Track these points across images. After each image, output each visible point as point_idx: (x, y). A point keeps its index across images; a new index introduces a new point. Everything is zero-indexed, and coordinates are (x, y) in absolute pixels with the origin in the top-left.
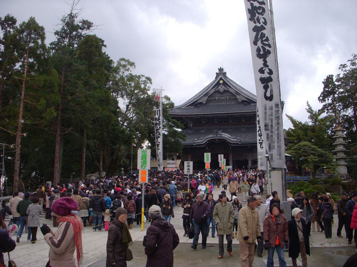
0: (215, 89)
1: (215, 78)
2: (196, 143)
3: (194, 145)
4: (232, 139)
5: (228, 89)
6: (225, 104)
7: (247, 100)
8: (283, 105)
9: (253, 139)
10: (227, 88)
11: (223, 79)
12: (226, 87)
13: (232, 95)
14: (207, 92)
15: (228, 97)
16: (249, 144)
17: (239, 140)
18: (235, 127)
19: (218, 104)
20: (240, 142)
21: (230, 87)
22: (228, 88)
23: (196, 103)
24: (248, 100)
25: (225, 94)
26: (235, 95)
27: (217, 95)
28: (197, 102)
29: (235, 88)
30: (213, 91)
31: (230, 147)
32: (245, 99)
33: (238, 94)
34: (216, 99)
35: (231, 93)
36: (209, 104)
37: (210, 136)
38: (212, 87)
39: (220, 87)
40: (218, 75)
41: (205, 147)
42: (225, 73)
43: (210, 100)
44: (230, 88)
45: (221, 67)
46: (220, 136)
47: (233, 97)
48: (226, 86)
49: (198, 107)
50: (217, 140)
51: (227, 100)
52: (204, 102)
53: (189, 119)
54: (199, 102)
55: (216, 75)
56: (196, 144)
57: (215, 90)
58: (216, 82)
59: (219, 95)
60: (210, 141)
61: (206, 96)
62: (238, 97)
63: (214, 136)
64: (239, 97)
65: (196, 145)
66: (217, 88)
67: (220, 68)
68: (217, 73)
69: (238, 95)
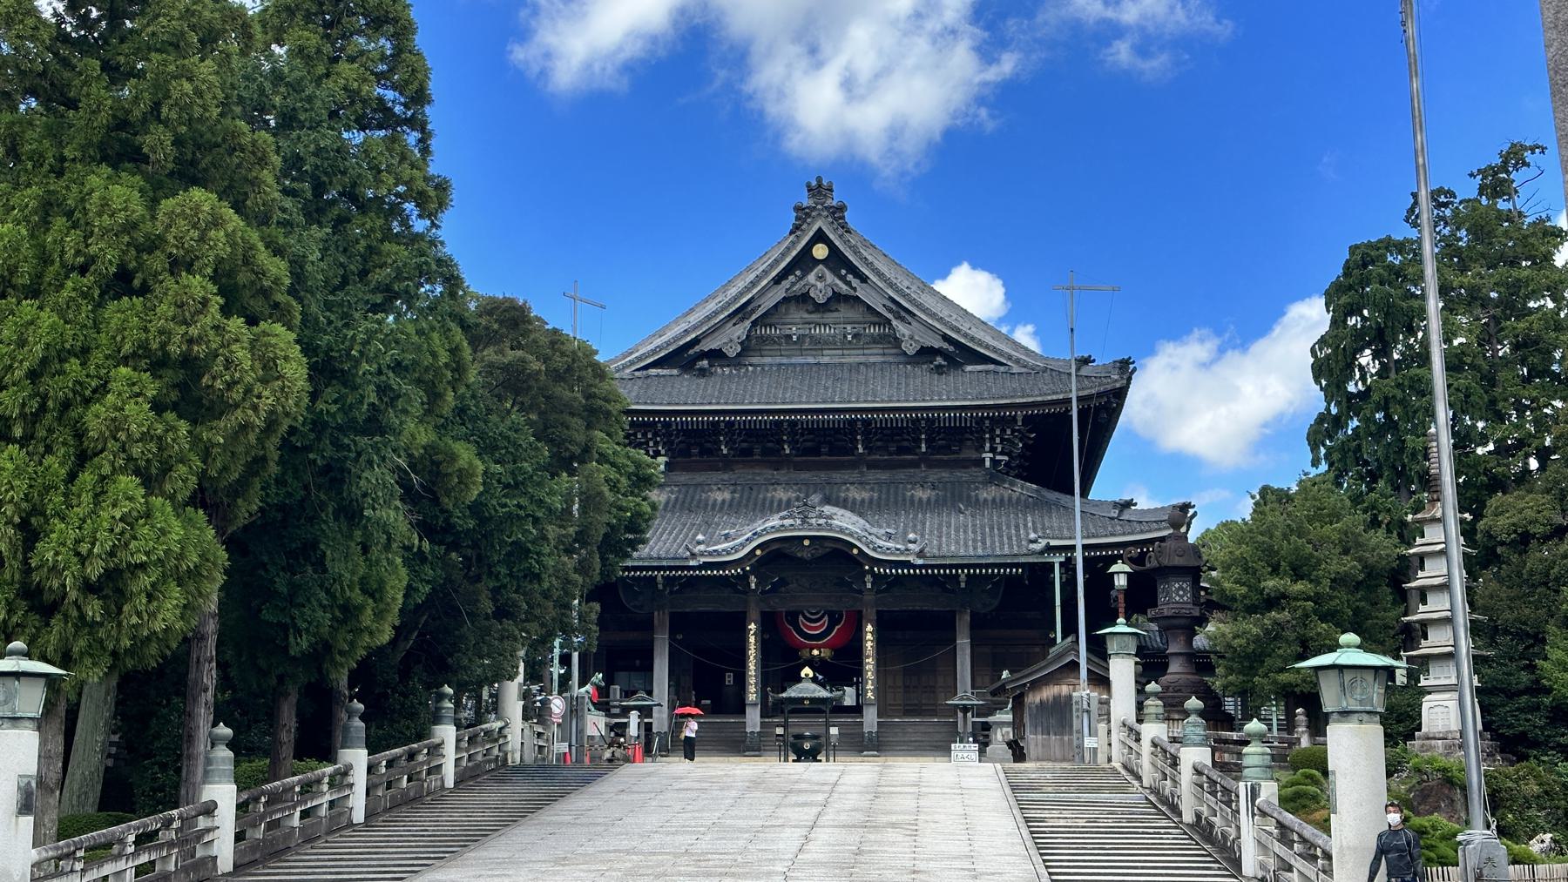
0: (786, 284)
1: (791, 233)
2: (702, 554)
3: (692, 563)
4: (881, 543)
6: (837, 360)
7: (945, 346)
8: (1129, 379)
9: (984, 543)
10: (848, 284)
11: (832, 237)
13: (876, 319)
15: (849, 328)
16: (962, 566)
17: (911, 546)
18: (884, 476)
19: (800, 360)
20: (921, 554)
21: (864, 279)
22: (855, 282)
23: (691, 352)
24: (951, 349)
25: (835, 314)
27: (797, 314)
28: (697, 349)
29: (891, 285)
30: (779, 293)
31: (868, 578)
32: (938, 343)
33: (902, 313)
34: (789, 337)
35: (869, 307)
36: (755, 360)
37: (774, 525)
38: (774, 274)
39: (811, 278)
40: (803, 214)
41: (744, 577)
42: (841, 208)
43: (764, 340)
45: (819, 179)
46: (822, 521)
47: (874, 331)
48: (843, 272)
49: (703, 373)
50: (806, 543)
51: (844, 345)
52: (732, 351)
53: (655, 434)
54: (707, 346)
55: (797, 218)
56: (703, 560)
58: (794, 253)
61: (742, 320)
62: (901, 328)
63: (790, 521)
64: (907, 333)
65: (700, 567)
66: (801, 279)
67: (814, 183)
68: (798, 209)
69: (902, 319)
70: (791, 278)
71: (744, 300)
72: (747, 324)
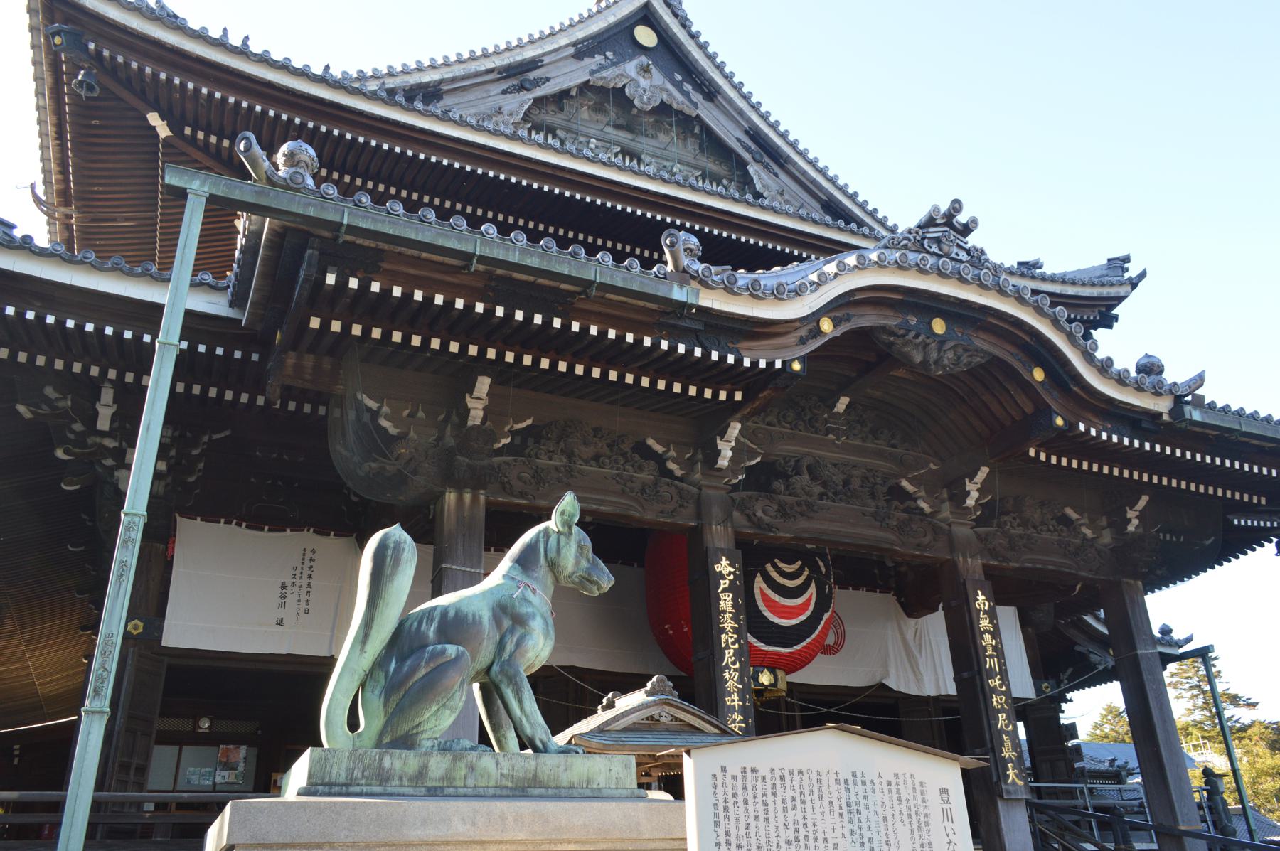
5: (696, 105)
10: (686, 94)
12: (678, 86)
13: (712, 166)
14: (534, 64)
21: (711, 93)
22: (696, 97)
26: (743, 164)
35: (712, 143)
38: (580, 34)
44: (707, 104)
48: (678, 77)
57: (592, 72)
59: (609, 130)
60: (867, 319)
66: (614, 64)
70: (599, 58)
71: (529, 53)
72: (527, 98)
